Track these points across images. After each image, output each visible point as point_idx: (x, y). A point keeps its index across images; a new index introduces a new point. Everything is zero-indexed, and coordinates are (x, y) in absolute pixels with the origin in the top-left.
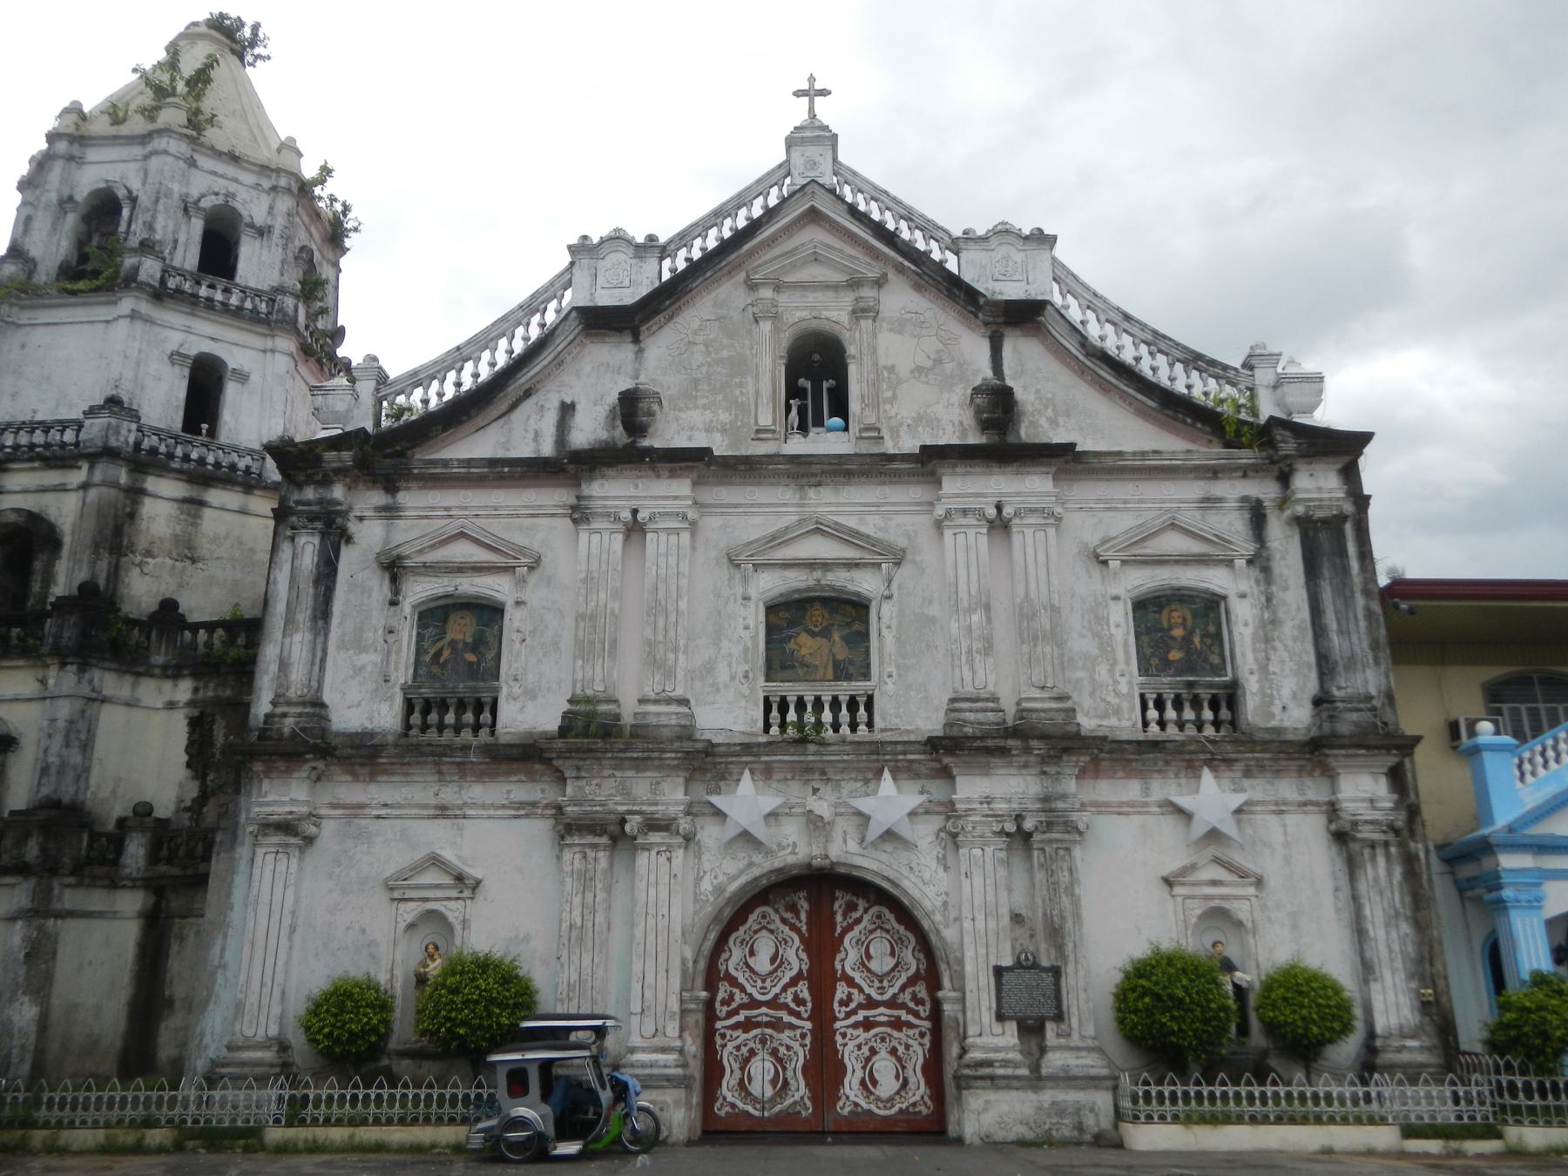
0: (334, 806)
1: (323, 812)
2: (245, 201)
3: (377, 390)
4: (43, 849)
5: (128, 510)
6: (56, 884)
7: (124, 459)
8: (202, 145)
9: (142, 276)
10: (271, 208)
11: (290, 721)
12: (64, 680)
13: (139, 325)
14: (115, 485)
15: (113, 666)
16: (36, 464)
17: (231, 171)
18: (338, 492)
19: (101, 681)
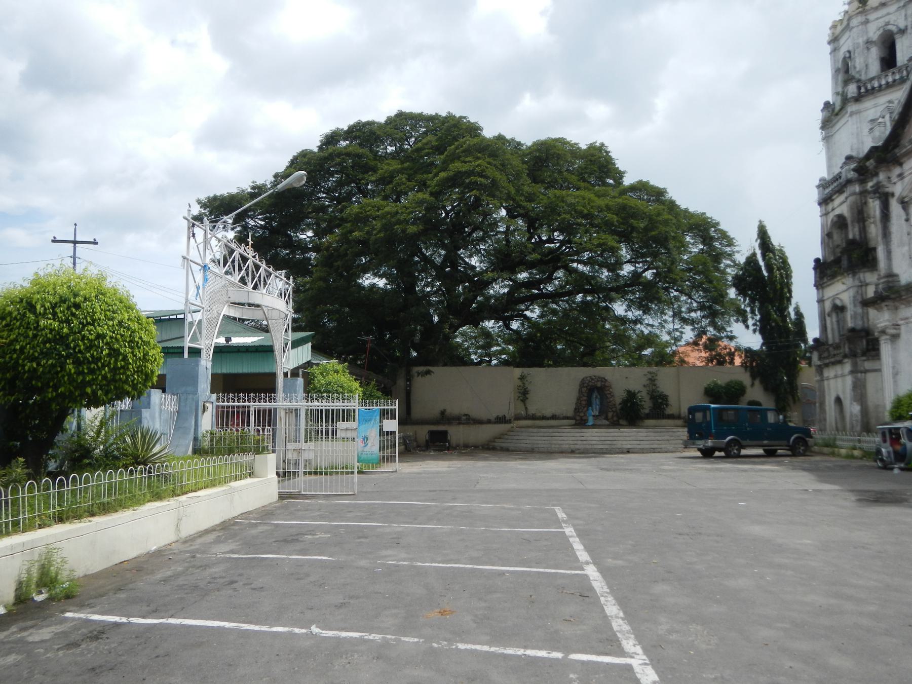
0: (902, 319)
1: (900, 322)
2: (895, 21)
3: (891, 117)
4: (850, 348)
5: (863, 201)
6: (858, 360)
7: (855, 181)
8: (868, 11)
9: (850, 95)
10: (906, 15)
11: (881, 286)
12: (849, 281)
13: (854, 117)
14: (854, 194)
15: (865, 270)
16: (837, 195)
17: (884, 11)
18: (882, 176)
19: (864, 277)
